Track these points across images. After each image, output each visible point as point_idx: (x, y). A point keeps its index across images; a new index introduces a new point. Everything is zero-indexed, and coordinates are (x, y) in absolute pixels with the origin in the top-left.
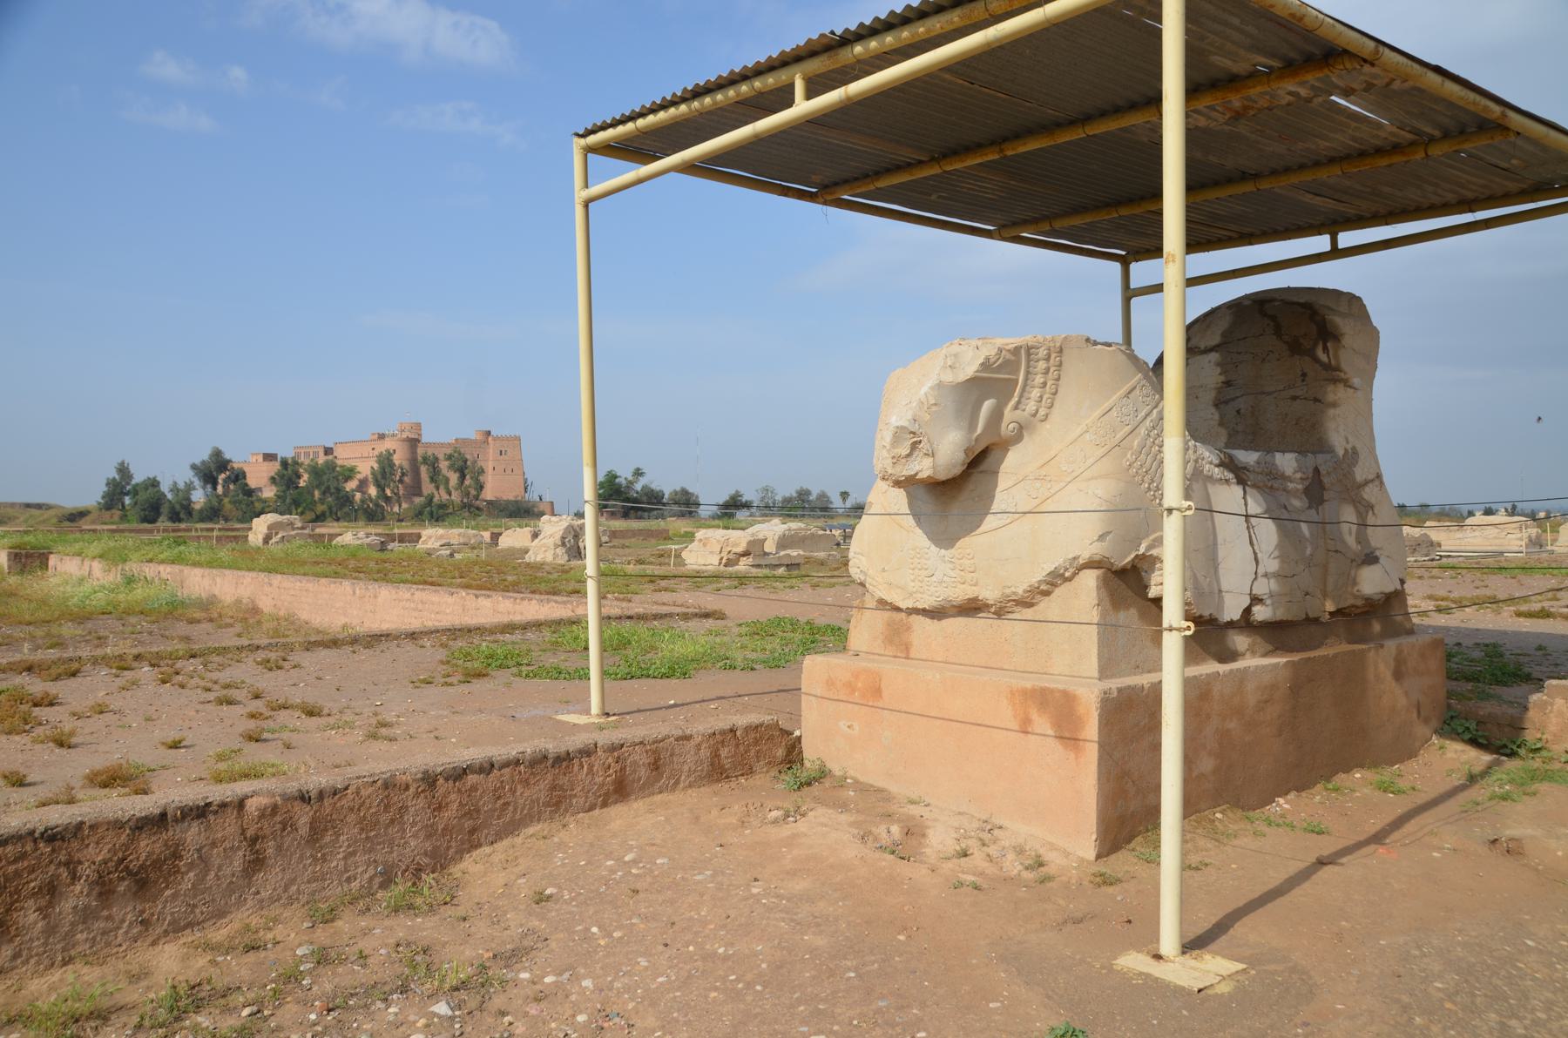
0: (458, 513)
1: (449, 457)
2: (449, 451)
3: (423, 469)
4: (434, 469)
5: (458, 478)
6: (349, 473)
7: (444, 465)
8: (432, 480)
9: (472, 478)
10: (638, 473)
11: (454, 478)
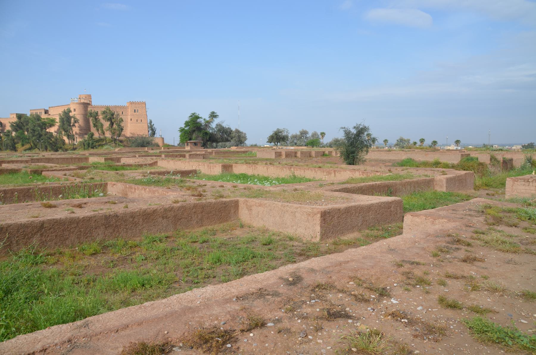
0: (109, 144)
1: (104, 113)
2: (103, 109)
3: (91, 119)
4: (96, 119)
5: (109, 125)
6: (51, 123)
7: (101, 117)
8: (95, 126)
9: (116, 124)
10: (213, 115)
11: (106, 124)
